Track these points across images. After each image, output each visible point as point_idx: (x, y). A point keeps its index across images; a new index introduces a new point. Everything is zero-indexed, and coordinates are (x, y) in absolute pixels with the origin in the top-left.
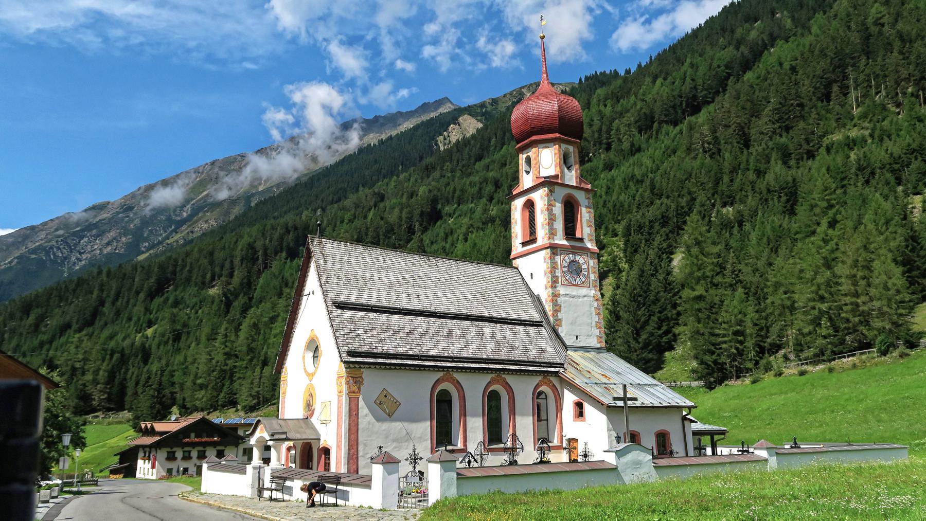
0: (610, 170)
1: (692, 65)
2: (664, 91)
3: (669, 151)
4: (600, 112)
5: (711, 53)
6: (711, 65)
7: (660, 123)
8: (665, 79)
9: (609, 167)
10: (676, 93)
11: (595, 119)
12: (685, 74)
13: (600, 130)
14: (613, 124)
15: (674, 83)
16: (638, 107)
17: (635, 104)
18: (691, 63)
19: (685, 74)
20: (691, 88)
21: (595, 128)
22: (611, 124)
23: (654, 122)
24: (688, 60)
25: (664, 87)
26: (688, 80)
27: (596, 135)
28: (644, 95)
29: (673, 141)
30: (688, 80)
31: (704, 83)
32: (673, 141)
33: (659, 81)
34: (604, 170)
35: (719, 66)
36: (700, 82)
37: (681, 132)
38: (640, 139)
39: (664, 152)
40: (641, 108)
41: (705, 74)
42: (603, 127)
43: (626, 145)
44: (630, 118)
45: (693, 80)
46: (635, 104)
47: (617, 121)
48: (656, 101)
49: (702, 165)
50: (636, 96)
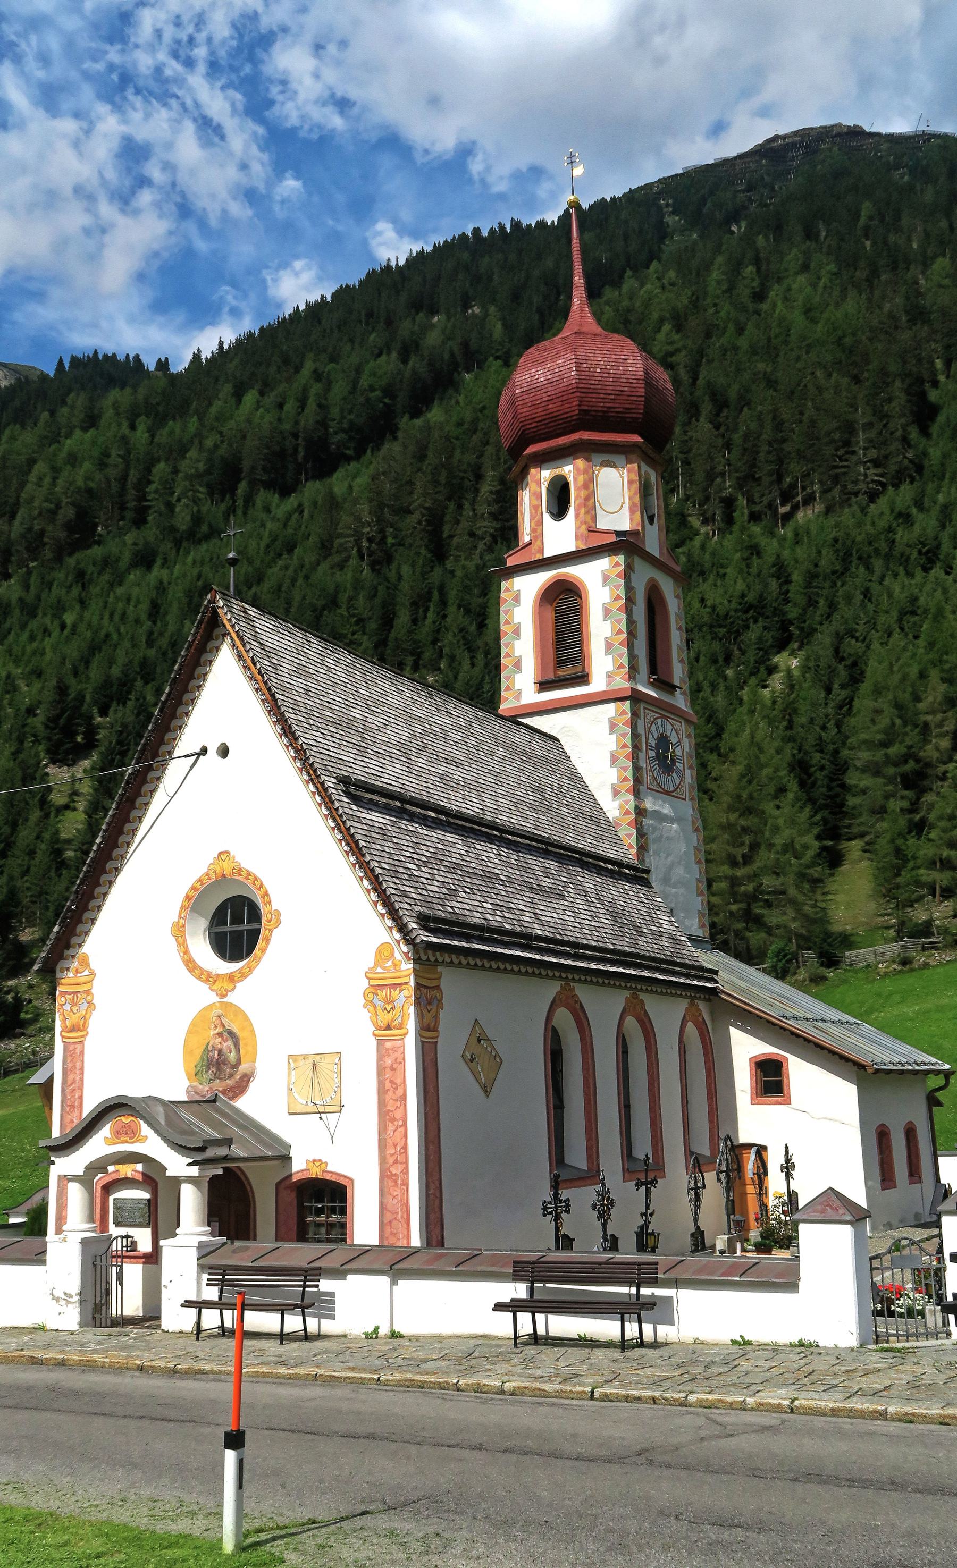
0: (149, 566)
1: (317, 376)
2: (262, 417)
3: (278, 544)
4: (124, 440)
5: (355, 359)
6: (355, 383)
7: (253, 484)
8: (262, 393)
9: (145, 559)
10: (287, 427)
11: (114, 453)
12: (305, 390)
13: (123, 479)
14: (155, 471)
15: (281, 406)
16: (209, 443)
17: (199, 436)
18: (315, 371)
19: (305, 390)
20: (317, 422)
21: (113, 473)
22: (148, 470)
23: (239, 480)
24: (309, 366)
25: (261, 410)
26: (311, 405)
27: (115, 488)
28: (217, 419)
29: (285, 525)
30: (311, 405)
31: (343, 417)
32: (285, 525)
33: (250, 398)
34: (134, 565)
35: (372, 389)
36: (335, 412)
37: (300, 509)
38: (213, 510)
39: (268, 546)
40: (216, 446)
41: (344, 399)
42: (132, 472)
43: (182, 519)
44: (193, 461)
45: (320, 406)
46: (199, 436)
47: (162, 465)
48: (244, 437)
49: (357, 584)
50: (200, 419)
